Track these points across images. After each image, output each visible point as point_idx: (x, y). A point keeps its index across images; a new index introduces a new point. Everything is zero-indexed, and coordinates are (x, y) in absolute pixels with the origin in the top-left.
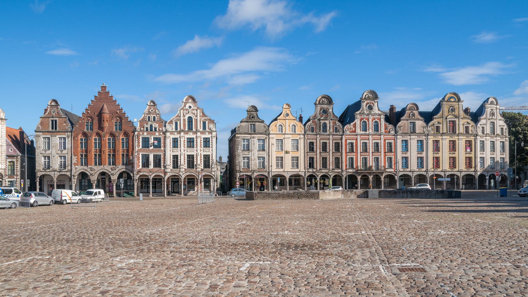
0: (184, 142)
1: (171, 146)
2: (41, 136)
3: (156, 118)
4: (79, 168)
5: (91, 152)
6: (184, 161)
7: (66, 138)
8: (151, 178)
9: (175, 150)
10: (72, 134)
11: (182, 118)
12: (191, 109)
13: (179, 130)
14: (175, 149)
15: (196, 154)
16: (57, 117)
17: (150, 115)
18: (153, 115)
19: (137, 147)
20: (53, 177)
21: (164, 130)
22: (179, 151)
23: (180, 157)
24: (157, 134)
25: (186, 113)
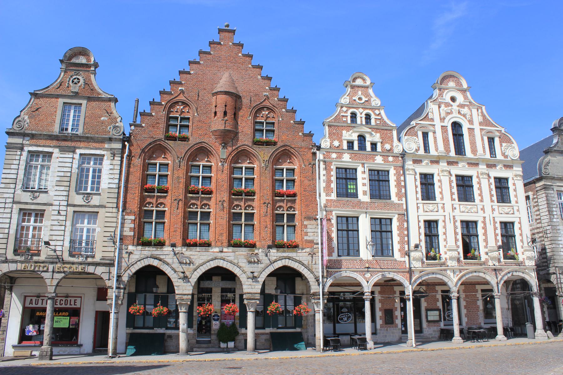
0: (450, 185)
1: (419, 195)
2: (26, 149)
3: (373, 117)
4: (139, 253)
5: (180, 203)
6: (456, 238)
7: (105, 158)
8: (367, 288)
9: (431, 207)
10: (124, 147)
11: (438, 124)
12: (457, 103)
13: (433, 152)
14: (430, 205)
15: (483, 220)
16: (83, 98)
17: (357, 108)
18: (365, 109)
19: (323, 194)
20: (48, 282)
21: (398, 150)
22: (441, 211)
23: (445, 227)
24: (379, 159)
25: (448, 114)
